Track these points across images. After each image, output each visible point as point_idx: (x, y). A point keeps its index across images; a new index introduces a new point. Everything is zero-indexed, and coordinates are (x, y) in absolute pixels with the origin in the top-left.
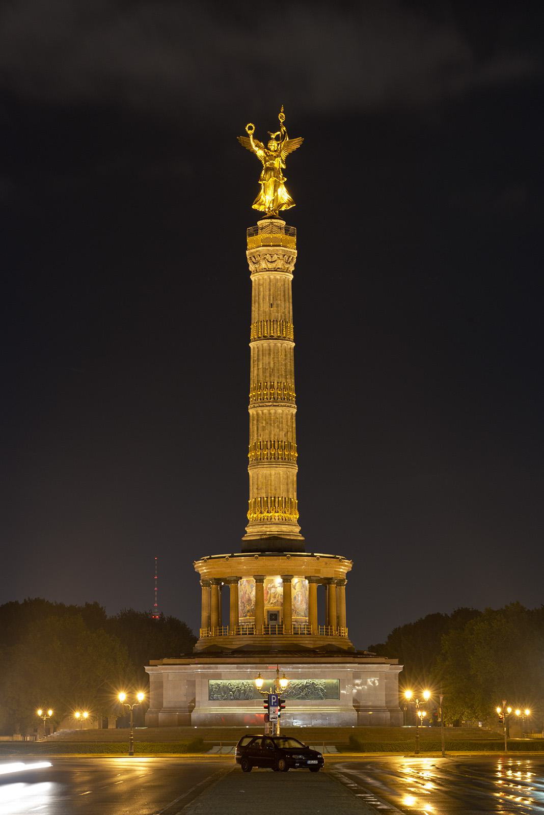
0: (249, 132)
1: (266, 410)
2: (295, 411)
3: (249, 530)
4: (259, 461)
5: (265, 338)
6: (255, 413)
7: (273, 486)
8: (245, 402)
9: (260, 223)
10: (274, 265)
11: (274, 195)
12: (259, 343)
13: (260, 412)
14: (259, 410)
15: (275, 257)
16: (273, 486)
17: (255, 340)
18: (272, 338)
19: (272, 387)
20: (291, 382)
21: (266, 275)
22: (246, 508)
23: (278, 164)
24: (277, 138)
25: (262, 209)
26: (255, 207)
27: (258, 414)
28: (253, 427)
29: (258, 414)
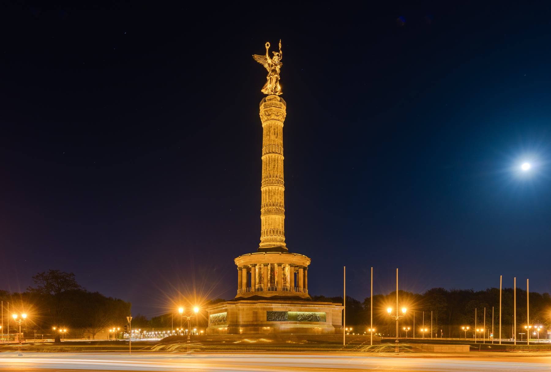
0: (267, 48)
1: (274, 187)
2: (283, 189)
3: (261, 244)
4: (269, 212)
5: (273, 153)
6: (267, 189)
7: (272, 223)
8: (260, 185)
9: (267, 98)
10: (277, 118)
11: (272, 87)
12: (267, 155)
13: (270, 188)
14: (267, 188)
15: (279, 114)
16: (272, 223)
17: (265, 154)
18: (276, 153)
19: (277, 177)
20: (282, 176)
21: (273, 122)
22: (260, 235)
23: (278, 68)
24: (278, 55)
25: (266, 93)
26: (263, 91)
27: (269, 189)
28: (263, 196)
29: (269, 189)
